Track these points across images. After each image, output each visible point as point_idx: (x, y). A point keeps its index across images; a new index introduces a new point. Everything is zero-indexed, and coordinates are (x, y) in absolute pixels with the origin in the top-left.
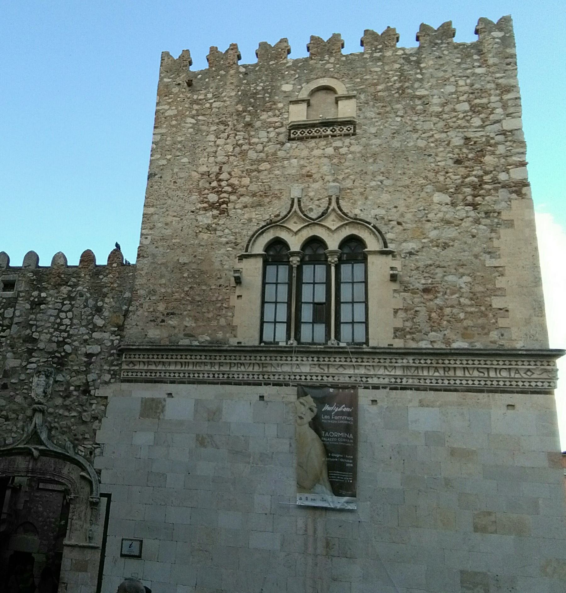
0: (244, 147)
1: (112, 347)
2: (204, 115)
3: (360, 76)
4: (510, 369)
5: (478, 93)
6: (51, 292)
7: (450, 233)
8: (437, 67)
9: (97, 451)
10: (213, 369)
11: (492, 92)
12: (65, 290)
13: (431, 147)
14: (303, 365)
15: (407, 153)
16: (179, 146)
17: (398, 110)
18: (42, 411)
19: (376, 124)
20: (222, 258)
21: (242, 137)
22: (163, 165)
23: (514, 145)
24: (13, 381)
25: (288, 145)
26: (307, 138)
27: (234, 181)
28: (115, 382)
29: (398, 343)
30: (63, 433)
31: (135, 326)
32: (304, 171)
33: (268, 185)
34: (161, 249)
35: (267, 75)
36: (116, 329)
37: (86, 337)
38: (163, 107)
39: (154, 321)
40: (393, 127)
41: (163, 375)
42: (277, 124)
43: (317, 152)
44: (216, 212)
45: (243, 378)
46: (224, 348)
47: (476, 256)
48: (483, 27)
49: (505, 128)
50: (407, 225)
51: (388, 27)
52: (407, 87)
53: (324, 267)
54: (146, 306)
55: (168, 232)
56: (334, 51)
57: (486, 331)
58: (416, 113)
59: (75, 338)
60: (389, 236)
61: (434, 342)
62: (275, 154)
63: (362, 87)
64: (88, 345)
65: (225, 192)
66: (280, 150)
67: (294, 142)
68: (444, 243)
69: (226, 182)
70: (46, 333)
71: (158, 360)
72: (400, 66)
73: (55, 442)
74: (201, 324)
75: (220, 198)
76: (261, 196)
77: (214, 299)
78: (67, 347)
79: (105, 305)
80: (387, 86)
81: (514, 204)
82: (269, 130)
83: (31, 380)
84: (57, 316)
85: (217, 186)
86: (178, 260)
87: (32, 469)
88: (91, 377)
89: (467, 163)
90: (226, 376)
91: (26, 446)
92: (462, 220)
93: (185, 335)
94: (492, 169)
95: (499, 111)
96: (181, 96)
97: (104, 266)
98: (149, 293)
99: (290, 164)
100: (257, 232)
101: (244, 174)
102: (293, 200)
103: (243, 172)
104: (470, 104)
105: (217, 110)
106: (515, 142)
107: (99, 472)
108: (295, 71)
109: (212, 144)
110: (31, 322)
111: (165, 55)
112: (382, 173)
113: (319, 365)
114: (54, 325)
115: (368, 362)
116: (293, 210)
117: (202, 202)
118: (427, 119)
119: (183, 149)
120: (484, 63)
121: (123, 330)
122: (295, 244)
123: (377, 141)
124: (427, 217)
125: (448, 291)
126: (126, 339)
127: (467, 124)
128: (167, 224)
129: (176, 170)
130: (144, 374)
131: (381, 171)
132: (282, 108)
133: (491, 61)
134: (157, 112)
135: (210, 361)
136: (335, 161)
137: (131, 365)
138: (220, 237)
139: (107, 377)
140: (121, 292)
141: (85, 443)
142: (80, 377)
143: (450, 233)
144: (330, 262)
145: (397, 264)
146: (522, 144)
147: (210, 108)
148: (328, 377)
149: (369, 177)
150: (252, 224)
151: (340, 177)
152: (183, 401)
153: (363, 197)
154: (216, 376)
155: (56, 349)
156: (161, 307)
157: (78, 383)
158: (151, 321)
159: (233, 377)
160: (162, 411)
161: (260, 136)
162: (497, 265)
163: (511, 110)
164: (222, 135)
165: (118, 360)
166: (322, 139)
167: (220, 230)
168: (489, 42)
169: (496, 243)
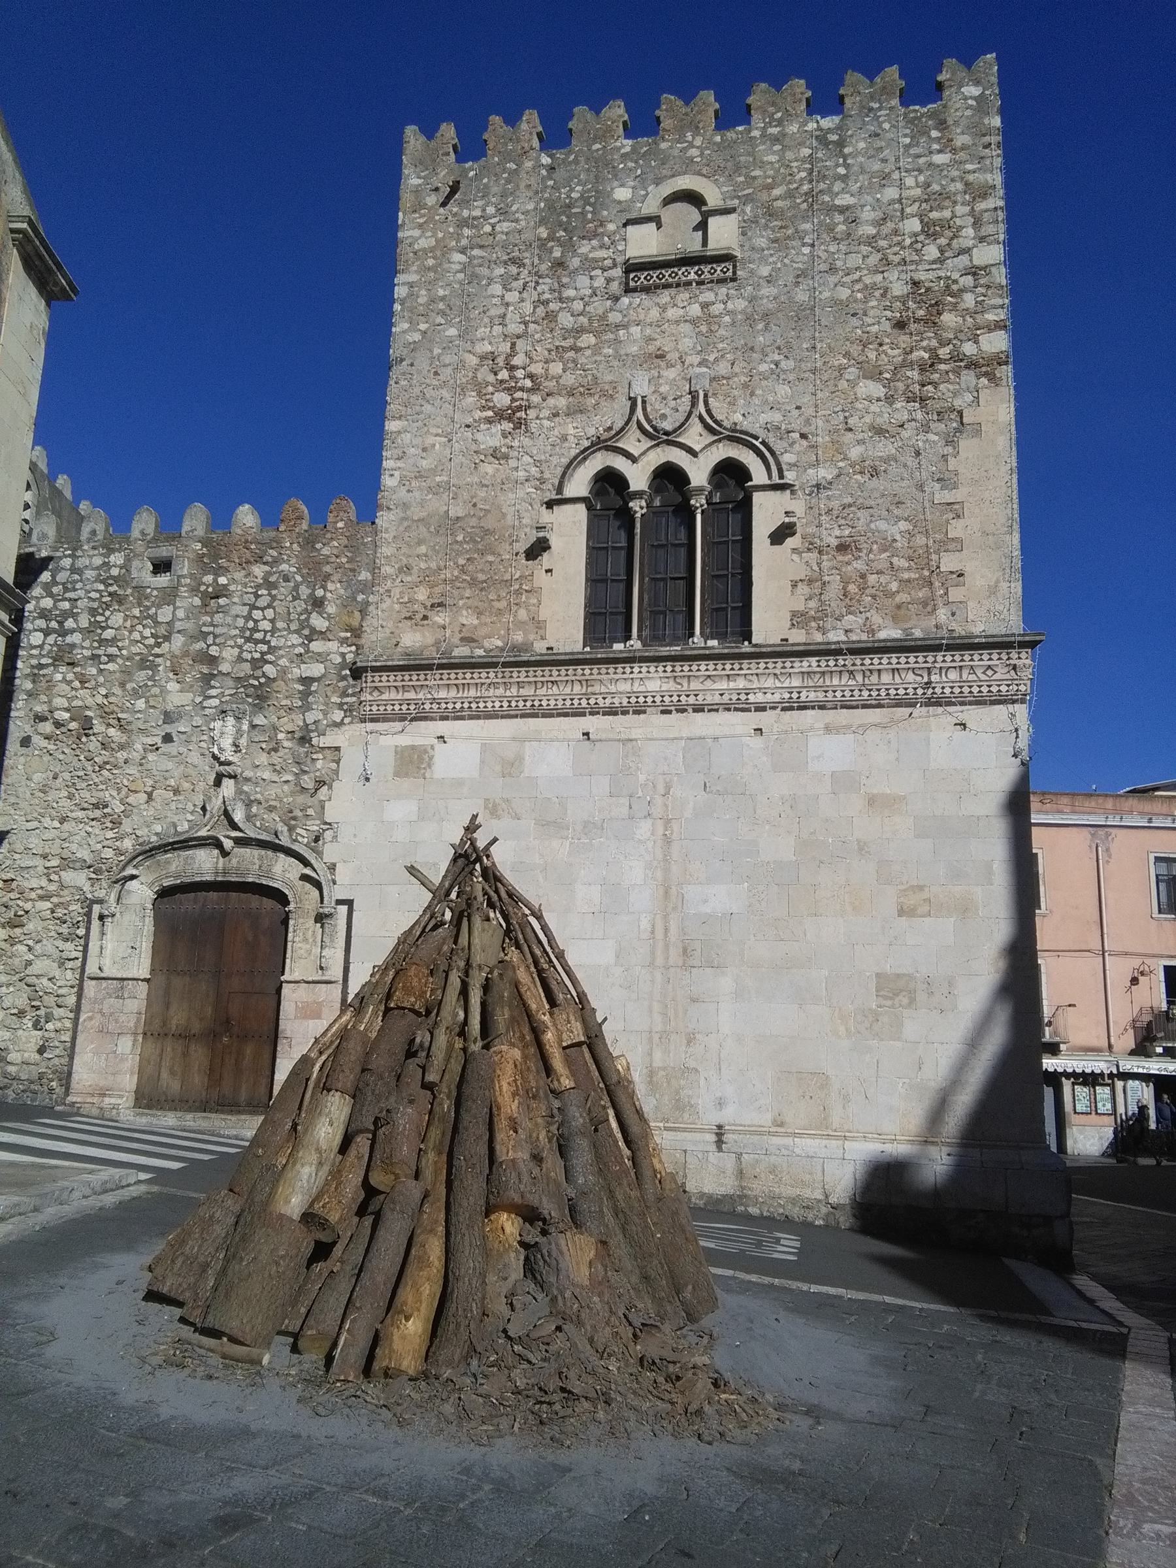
1: (343, 665)
17: (806, 232)
19: (771, 260)
24: (183, 730)
36: (349, 635)
39: (410, 618)
40: (795, 265)
46: (525, 659)
54: (396, 593)
55: (425, 464)
58: (835, 239)
59: (281, 652)
78: (270, 670)
79: (329, 595)
84: (249, 617)
98: (400, 570)
100: (575, 458)
102: (633, 401)
110: (204, 629)
114: (244, 632)
118: (853, 249)
121: (358, 636)
122: (638, 478)
123: (774, 291)
126: (366, 650)
133: (961, 140)
156: (422, 594)
168: (958, 106)
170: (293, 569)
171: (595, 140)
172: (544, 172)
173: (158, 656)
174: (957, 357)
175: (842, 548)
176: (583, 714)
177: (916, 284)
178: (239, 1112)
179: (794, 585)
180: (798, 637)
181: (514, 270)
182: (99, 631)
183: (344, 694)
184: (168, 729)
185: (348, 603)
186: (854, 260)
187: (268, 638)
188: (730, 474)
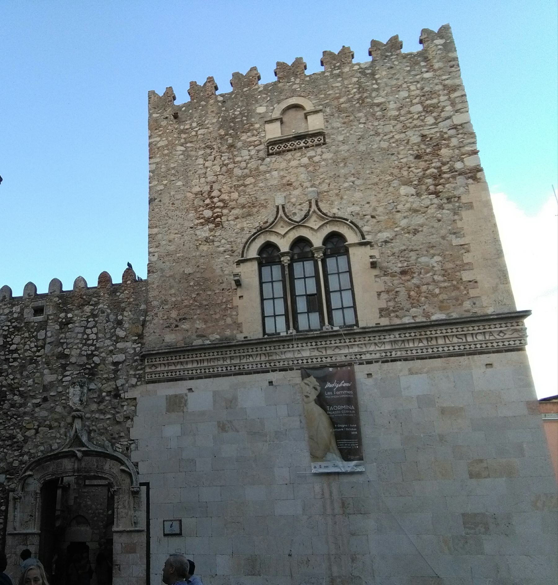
0: (230, 166)
1: (135, 354)
2: (191, 142)
3: (323, 92)
4: (484, 332)
5: (428, 95)
6: (76, 312)
7: (419, 220)
8: (390, 76)
9: (133, 446)
10: (225, 363)
11: (441, 92)
12: (88, 309)
13: (393, 147)
14: (303, 350)
15: (372, 155)
16: (173, 172)
17: (361, 118)
18: (81, 417)
19: (343, 132)
20: (222, 266)
21: (226, 158)
22: (161, 190)
23: (466, 137)
24: (52, 394)
25: (268, 159)
26: (284, 151)
27: (225, 197)
28: (141, 384)
29: (385, 322)
30: (101, 434)
31: (153, 334)
32: (285, 181)
33: (255, 197)
34: (167, 263)
35: (242, 101)
36: (137, 338)
38: (155, 139)
39: (169, 327)
40: (357, 134)
41: (182, 373)
42: (256, 142)
43: (294, 163)
44: (212, 226)
45: (252, 367)
46: (233, 344)
47: (443, 238)
48: (426, 37)
49: (455, 123)
50: (380, 218)
51: (343, 47)
52: (365, 97)
53: (312, 262)
54: (160, 314)
55: (172, 248)
56: (298, 73)
57: (460, 302)
58: (377, 119)
59: (102, 350)
60: (365, 229)
61: (416, 316)
62: (257, 169)
63: (326, 101)
64: (114, 354)
65: (218, 207)
66: (261, 165)
67: (273, 156)
68: (414, 229)
69: (217, 198)
70: (76, 349)
71: (176, 361)
72: (357, 79)
73: (95, 443)
74: (210, 325)
75: (214, 213)
76: (249, 207)
78: (96, 359)
79: (125, 318)
80: (349, 98)
81: (471, 188)
82: (250, 148)
83: (67, 391)
84: (84, 333)
85: (210, 203)
86: (184, 271)
87: (78, 469)
88: (119, 383)
89: (426, 158)
90: (237, 368)
91: (70, 449)
92: (427, 207)
93: (198, 336)
94: (448, 160)
95: (449, 108)
96: (169, 127)
97: (120, 284)
99: (272, 176)
100: (249, 238)
101: (233, 190)
103: (231, 188)
104: (422, 106)
105: (202, 136)
106: (465, 134)
107: (136, 465)
108: (267, 94)
109: (201, 166)
110: (62, 341)
111: (152, 94)
112: (353, 174)
113: (318, 348)
115: (360, 341)
116: (279, 216)
117: (199, 218)
119: (177, 174)
120: (430, 68)
122: (284, 245)
123: (346, 147)
124: (396, 208)
125: (422, 271)
126: (146, 346)
127: (422, 123)
128: (170, 241)
129: (172, 193)
130: (165, 374)
131: (352, 173)
132: (259, 128)
133: (436, 66)
134: (150, 144)
135: (222, 356)
136: (311, 169)
137: (153, 368)
138: (218, 247)
140: (137, 305)
141: (121, 440)
142: (110, 383)
143: (419, 220)
144: (317, 257)
145: (375, 252)
146: (472, 135)
147: (197, 135)
148: (326, 358)
149: (342, 179)
150: (244, 232)
152: (202, 394)
153: (339, 198)
154: (229, 368)
155: (86, 361)
156: (174, 314)
157: (109, 389)
158: (166, 327)
159: (244, 368)
160: (186, 405)
161: (242, 155)
162: (463, 243)
163: (459, 106)
164: (209, 158)
165: (141, 365)
166: (297, 151)
167: (218, 241)
168: (433, 49)
169: (459, 224)
170: (106, 307)
173: (38, 356)
182: (8, 346)
183: (136, 369)
184: (45, 394)
187: (95, 343)
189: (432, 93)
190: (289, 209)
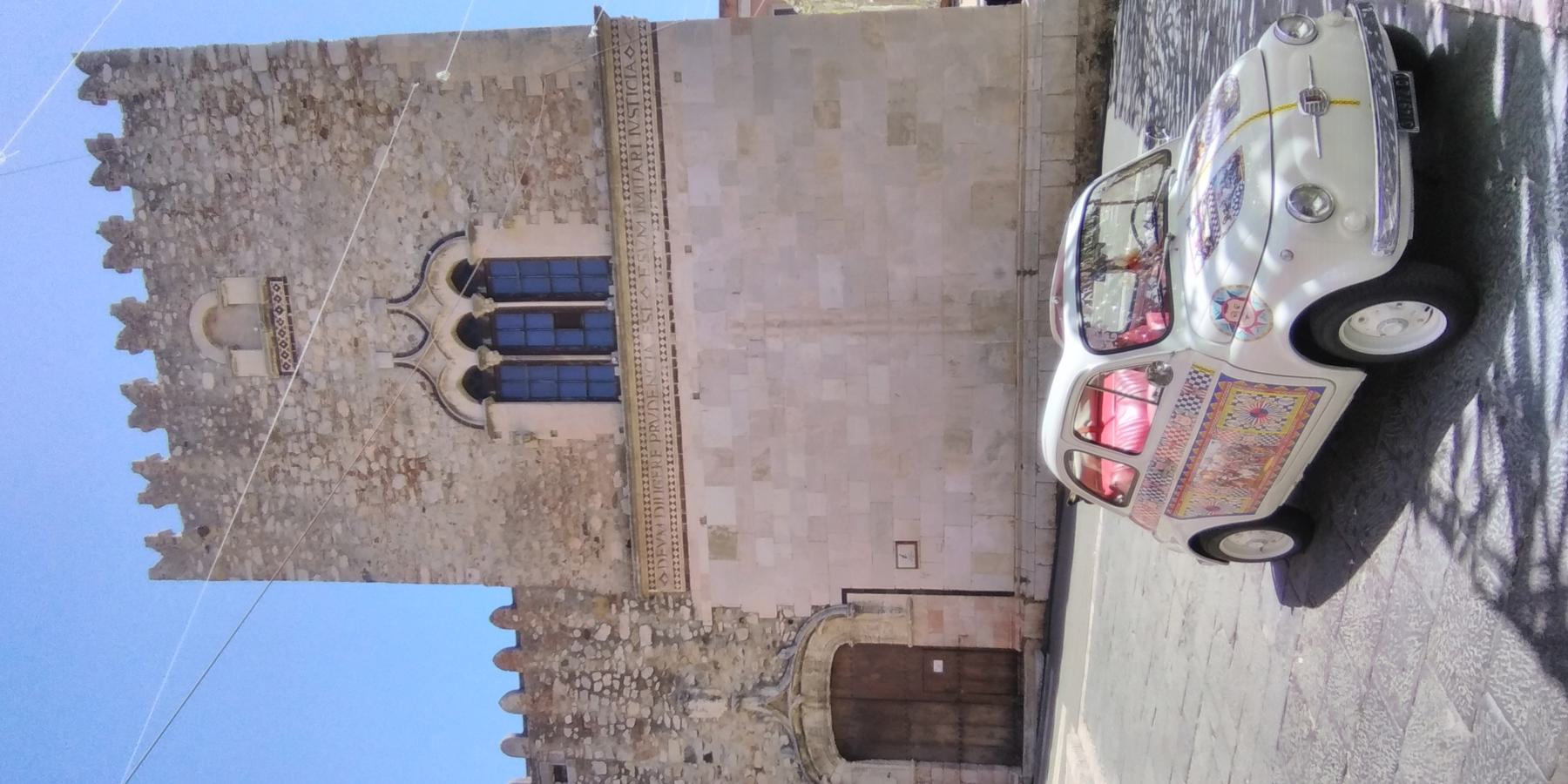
1: (641, 608)
8: (165, 162)
12: (559, 688)
17: (241, 217)
37: (629, 648)
48: (94, 92)
54: (575, 566)
77: (558, 470)
78: (647, 673)
98: (555, 563)
120: (157, 94)
139: (685, 611)
151: (356, 298)
156: (576, 544)
171: (159, 409)
172: (189, 452)
174: (351, 84)
175: (525, 181)
176: (677, 400)
177: (286, 121)
178: (1022, 676)
179: (559, 221)
180: (603, 217)
181: (280, 476)
184: (700, 759)
185: (586, 608)
186: (265, 175)
188: (462, 278)
189: (205, 96)
190: (401, 345)
